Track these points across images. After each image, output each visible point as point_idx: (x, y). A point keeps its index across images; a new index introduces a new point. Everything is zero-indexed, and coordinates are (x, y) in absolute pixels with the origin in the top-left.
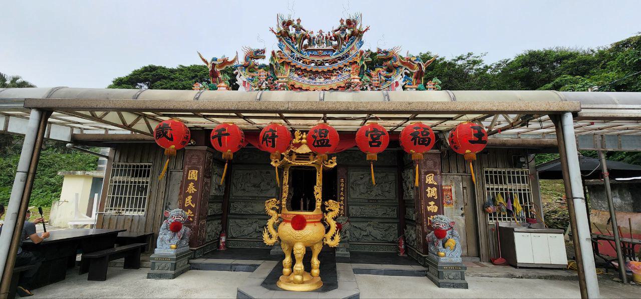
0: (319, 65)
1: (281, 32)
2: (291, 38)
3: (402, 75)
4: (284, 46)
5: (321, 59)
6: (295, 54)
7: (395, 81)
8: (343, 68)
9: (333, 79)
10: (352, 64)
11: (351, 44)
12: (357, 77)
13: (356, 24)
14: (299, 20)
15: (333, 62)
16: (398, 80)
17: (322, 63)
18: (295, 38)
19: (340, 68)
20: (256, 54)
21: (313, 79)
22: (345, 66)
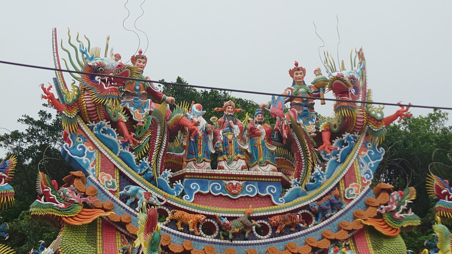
0: (236, 236)
1: (77, 102)
2: (115, 125)
4: (90, 156)
5: (240, 212)
6: (141, 191)
10: (356, 235)
13: (357, 92)
14: (140, 58)
17: (247, 227)
18: (131, 123)
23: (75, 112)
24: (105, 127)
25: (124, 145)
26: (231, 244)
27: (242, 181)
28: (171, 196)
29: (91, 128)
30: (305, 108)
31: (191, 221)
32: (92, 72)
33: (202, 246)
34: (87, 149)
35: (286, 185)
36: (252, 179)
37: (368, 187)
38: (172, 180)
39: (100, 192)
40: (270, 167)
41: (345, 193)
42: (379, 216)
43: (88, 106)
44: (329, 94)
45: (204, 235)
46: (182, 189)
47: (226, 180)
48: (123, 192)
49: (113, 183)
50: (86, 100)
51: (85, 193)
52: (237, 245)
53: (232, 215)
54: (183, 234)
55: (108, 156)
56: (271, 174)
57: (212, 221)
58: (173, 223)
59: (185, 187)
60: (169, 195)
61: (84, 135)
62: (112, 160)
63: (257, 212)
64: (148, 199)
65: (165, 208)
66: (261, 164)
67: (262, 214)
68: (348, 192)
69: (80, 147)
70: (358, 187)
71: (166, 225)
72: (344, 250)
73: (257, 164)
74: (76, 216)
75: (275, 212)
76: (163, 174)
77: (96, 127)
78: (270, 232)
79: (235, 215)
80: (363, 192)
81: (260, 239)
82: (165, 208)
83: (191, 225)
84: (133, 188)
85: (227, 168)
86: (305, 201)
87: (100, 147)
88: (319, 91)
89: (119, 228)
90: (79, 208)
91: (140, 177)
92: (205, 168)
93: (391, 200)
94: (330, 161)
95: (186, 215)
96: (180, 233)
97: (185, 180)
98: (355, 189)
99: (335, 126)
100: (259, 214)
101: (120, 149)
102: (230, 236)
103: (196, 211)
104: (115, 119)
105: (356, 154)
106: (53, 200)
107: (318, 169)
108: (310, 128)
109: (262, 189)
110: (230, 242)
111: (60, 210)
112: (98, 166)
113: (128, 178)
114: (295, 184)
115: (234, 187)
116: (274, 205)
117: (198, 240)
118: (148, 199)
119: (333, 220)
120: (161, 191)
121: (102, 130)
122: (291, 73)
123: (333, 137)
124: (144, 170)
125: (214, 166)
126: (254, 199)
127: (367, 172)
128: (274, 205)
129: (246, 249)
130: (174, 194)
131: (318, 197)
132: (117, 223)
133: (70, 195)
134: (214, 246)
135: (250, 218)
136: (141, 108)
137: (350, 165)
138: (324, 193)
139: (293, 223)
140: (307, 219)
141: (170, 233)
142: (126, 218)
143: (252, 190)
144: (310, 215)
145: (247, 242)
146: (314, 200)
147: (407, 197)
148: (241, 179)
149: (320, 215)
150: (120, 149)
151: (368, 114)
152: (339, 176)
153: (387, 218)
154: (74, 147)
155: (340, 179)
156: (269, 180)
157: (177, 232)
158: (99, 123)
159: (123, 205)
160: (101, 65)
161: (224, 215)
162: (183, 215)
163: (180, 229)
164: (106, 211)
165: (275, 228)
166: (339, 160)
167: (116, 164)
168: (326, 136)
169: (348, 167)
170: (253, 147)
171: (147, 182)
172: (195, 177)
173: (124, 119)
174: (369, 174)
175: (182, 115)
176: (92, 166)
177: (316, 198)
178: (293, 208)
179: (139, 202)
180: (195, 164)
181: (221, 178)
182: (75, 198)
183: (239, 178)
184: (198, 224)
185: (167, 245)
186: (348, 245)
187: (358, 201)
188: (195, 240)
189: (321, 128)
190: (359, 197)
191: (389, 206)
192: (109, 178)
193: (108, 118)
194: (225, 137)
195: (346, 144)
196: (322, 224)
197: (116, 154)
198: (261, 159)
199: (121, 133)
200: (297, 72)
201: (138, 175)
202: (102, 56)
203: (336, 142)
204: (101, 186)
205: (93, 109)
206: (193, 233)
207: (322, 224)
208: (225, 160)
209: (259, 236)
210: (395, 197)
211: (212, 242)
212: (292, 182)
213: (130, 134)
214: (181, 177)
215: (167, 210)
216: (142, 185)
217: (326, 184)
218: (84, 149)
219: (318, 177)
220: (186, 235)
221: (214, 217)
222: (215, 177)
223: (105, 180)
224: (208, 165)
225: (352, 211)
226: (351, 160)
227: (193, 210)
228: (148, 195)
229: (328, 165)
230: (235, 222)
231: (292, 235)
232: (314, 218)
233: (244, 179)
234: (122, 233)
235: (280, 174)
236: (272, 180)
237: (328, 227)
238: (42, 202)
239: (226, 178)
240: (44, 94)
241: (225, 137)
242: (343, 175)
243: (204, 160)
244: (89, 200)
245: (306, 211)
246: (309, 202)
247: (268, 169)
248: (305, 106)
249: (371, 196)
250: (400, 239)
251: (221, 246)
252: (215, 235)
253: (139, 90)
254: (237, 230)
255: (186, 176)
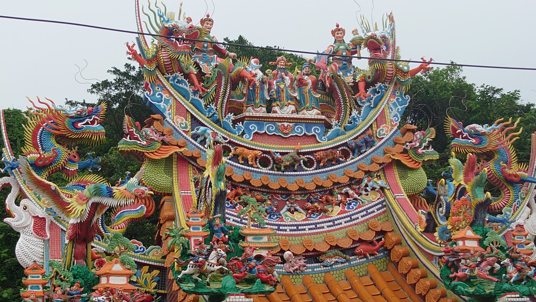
0: (287, 168)
1: (156, 57)
2: (187, 76)
3: (529, 205)
4: (167, 102)
5: (290, 149)
6: (209, 131)
7: (517, 222)
8: (360, 181)
9: (334, 216)
10: (385, 167)
11: (376, 106)
12: (469, 233)
13: (388, 49)
14: (207, 21)
15: (330, 159)
16: (520, 221)
17: (296, 161)
18: (201, 74)
19: (354, 182)
20: (74, 124)
21: (270, 213)
22: (368, 173)
23: (154, 66)
24: (179, 78)
25: (195, 93)
26: (283, 175)
27: (292, 123)
28: (234, 135)
29: (168, 79)
30: (344, 62)
31: (250, 156)
32: (169, 33)
33: (259, 177)
34: (164, 96)
35: (329, 126)
36: (301, 121)
37: (396, 128)
38: (235, 122)
39: (175, 131)
40: (315, 111)
41: (376, 132)
42: (405, 151)
43: (165, 60)
44: (365, 52)
45: (261, 167)
46: (242, 130)
47: (279, 122)
48: (194, 132)
49: (186, 125)
50: (163, 56)
51: (163, 132)
52: (288, 175)
53: (284, 151)
54: (243, 166)
55: (181, 102)
56: (316, 117)
57: (267, 156)
58: (235, 158)
59: (245, 128)
60: (232, 135)
61: (162, 85)
62: (185, 106)
63: (305, 149)
64: (214, 138)
65: (228, 145)
66: (307, 109)
67: (308, 150)
68: (379, 132)
69: (158, 95)
70: (388, 127)
71: (230, 159)
72: (375, 179)
73: (304, 108)
74: (156, 152)
75: (319, 149)
76: (227, 117)
77: (171, 78)
78: (315, 165)
79: (286, 151)
80: (392, 132)
81: (306, 171)
82: (228, 145)
83: (250, 159)
84: (202, 128)
85: (279, 112)
86: (344, 139)
87: (175, 95)
88: (356, 48)
89: (191, 162)
90: (159, 145)
91: (208, 119)
92: (262, 112)
93: (415, 139)
94: (365, 106)
95: (246, 150)
96: (241, 166)
97: (245, 122)
98: (385, 129)
99: (369, 77)
100: (306, 150)
101: (192, 96)
102: (282, 168)
103: (254, 147)
104: (187, 72)
105: (386, 101)
106: (137, 139)
107: (355, 113)
108: (349, 79)
109: (308, 129)
110: (282, 173)
111: (143, 146)
112: (173, 110)
113: (198, 121)
114: (336, 125)
115: (286, 128)
116: (319, 143)
117: (256, 172)
118: (214, 138)
119: (367, 155)
120: (225, 131)
121: (176, 80)
122: (333, 33)
123: (367, 86)
124: (211, 114)
125: (269, 111)
126: (301, 138)
127: (396, 116)
128: (319, 143)
129: (295, 178)
130: (236, 134)
131: (355, 136)
132: (189, 157)
133: (151, 135)
134: (269, 176)
135: (299, 154)
136: (208, 62)
137: (381, 110)
138: (360, 133)
139: (334, 158)
140: (346, 154)
141: (233, 165)
142: (197, 153)
143: (300, 130)
144: (348, 151)
145: (296, 173)
146: (351, 138)
147: (428, 136)
148: (291, 121)
149: (356, 151)
150: (192, 96)
151: (397, 67)
152: (372, 119)
153: (411, 154)
154: (154, 94)
155: (373, 121)
156: (314, 122)
157: (239, 165)
158: (174, 75)
159: (195, 142)
160: (175, 27)
161: (277, 151)
162: (243, 151)
163: (241, 162)
164: (180, 147)
165: (319, 162)
166: (372, 106)
167: (188, 109)
168: (362, 85)
169: (380, 111)
170: (301, 94)
171: (213, 124)
172: (253, 119)
173: (195, 71)
174: (397, 117)
175: (243, 68)
176: (169, 110)
177: (353, 137)
178: (334, 145)
179: (207, 140)
180: (253, 109)
181: (275, 120)
182: (155, 136)
183: (289, 121)
184: (256, 158)
185: (231, 176)
186: (379, 176)
187: (387, 140)
188: (253, 171)
189: (358, 79)
190: (388, 136)
191: (413, 143)
192: (182, 120)
193: (181, 71)
194: (278, 87)
195: (378, 92)
196: (358, 158)
197: (188, 100)
198: (308, 105)
199: (192, 83)
200: (338, 32)
201: (206, 118)
202: (176, 19)
203: (370, 90)
204: (176, 127)
205: (169, 63)
206: (252, 166)
207: (358, 158)
208: (278, 105)
209: (306, 168)
210: (418, 136)
211: (267, 173)
212: (334, 124)
213: (200, 84)
214: (242, 120)
215: (230, 147)
216: (210, 126)
217: (361, 125)
218: (162, 96)
219: (354, 119)
220: (246, 167)
221: (269, 153)
222: (270, 120)
223: (180, 122)
224: (264, 109)
225: (382, 147)
226: (383, 105)
227: (252, 147)
228: (215, 134)
229: (363, 109)
230: (286, 157)
231: (333, 168)
232: (351, 153)
233: (294, 121)
234: (193, 165)
235: (323, 117)
236: (316, 122)
237: (363, 161)
238: (128, 140)
239: (279, 120)
240: (129, 51)
241: (278, 87)
242: (375, 118)
243: (261, 106)
244: (167, 139)
245: (344, 148)
246: (347, 140)
247: (314, 113)
248: (345, 61)
249: (399, 135)
250: (422, 170)
251: (275, 177)
252: (270, 168)
253: (207, 47)
254: (288, 163)
255: (246, 119)
